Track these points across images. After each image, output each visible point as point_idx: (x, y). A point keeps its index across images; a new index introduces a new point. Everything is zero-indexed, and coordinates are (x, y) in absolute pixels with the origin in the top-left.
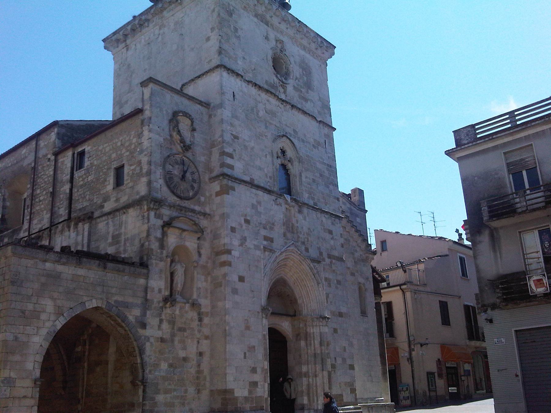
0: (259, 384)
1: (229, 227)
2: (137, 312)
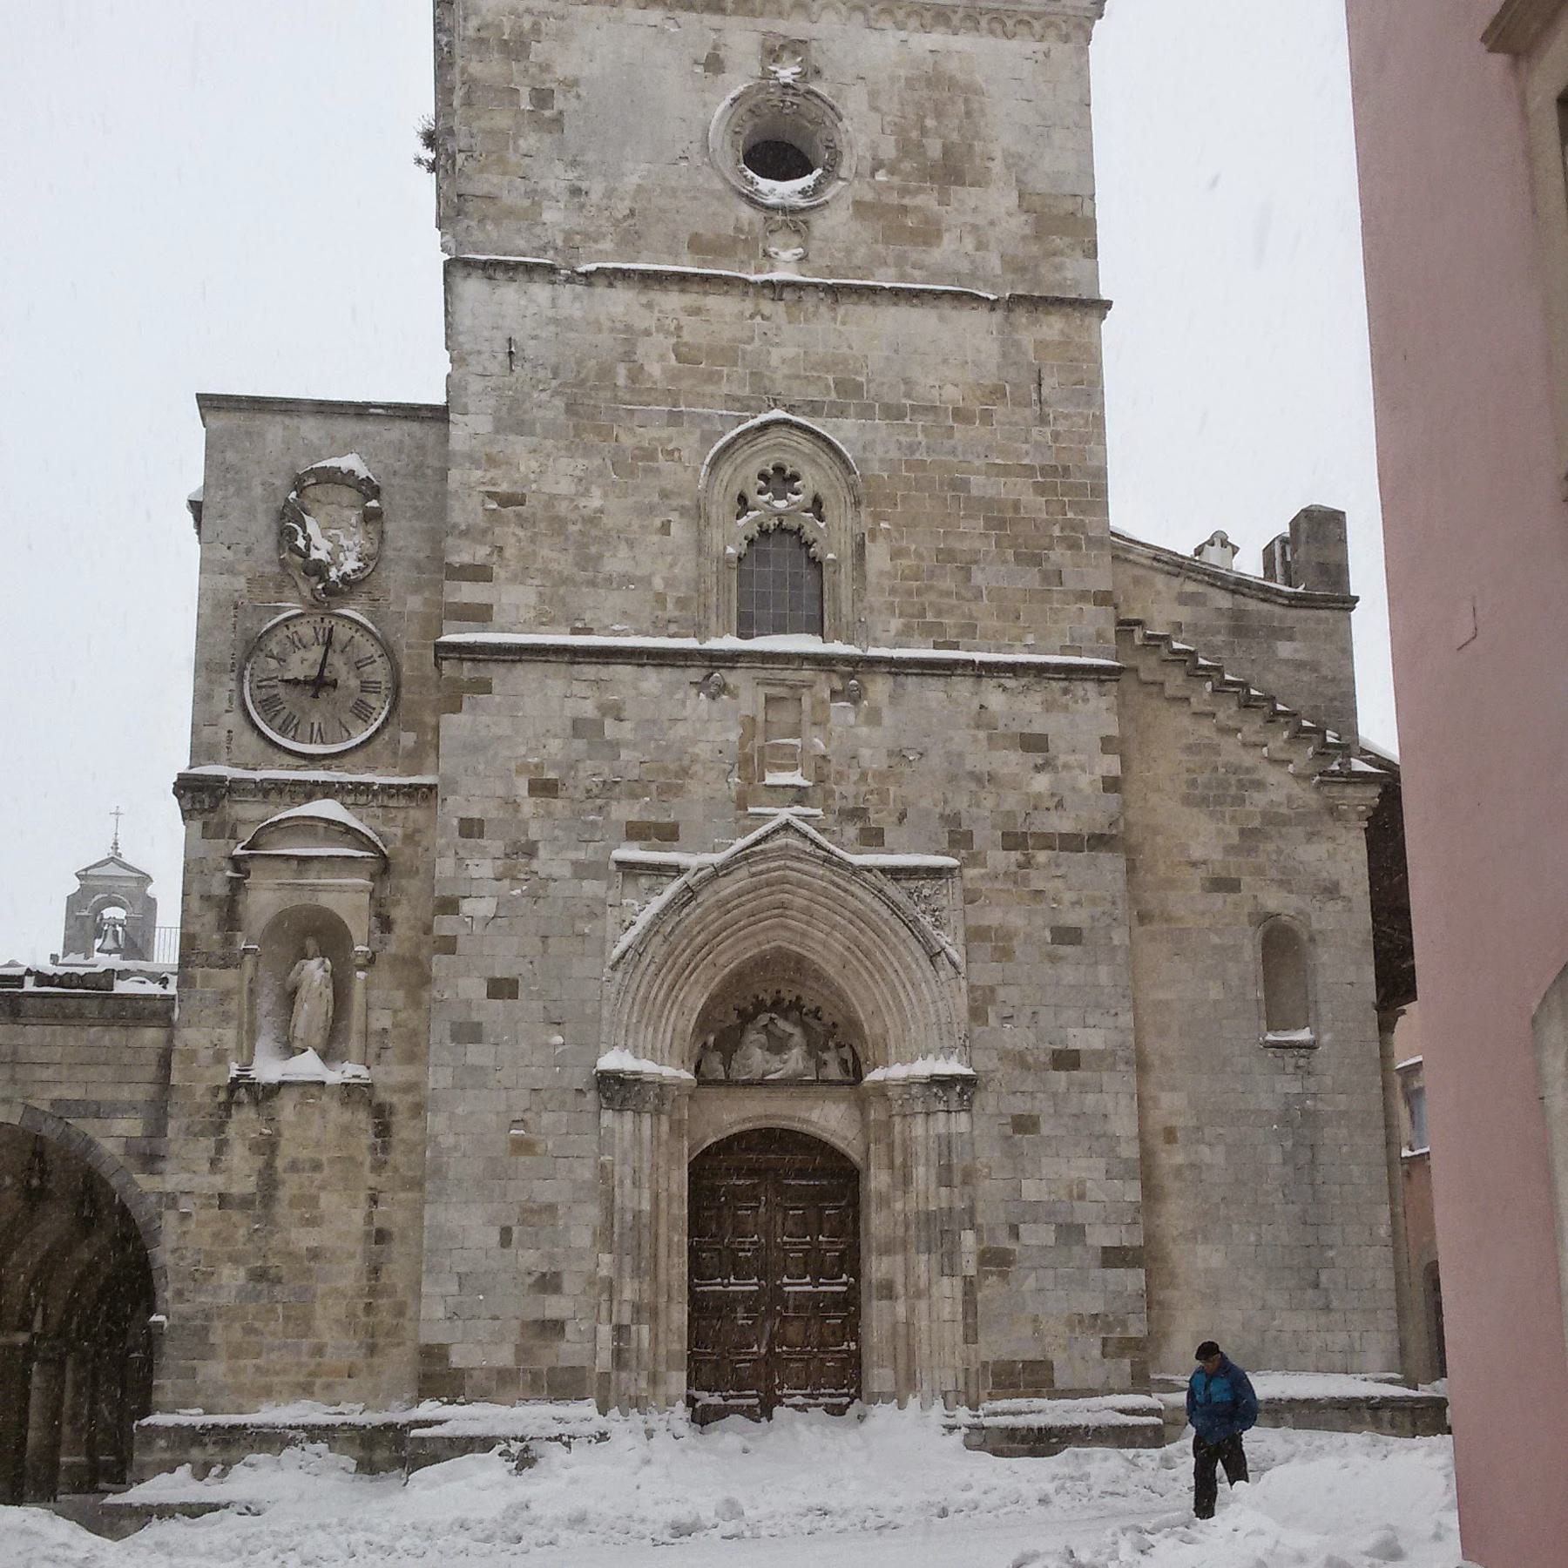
0: (569, 1328)
1: (455, 822)
2: (129, 1126)
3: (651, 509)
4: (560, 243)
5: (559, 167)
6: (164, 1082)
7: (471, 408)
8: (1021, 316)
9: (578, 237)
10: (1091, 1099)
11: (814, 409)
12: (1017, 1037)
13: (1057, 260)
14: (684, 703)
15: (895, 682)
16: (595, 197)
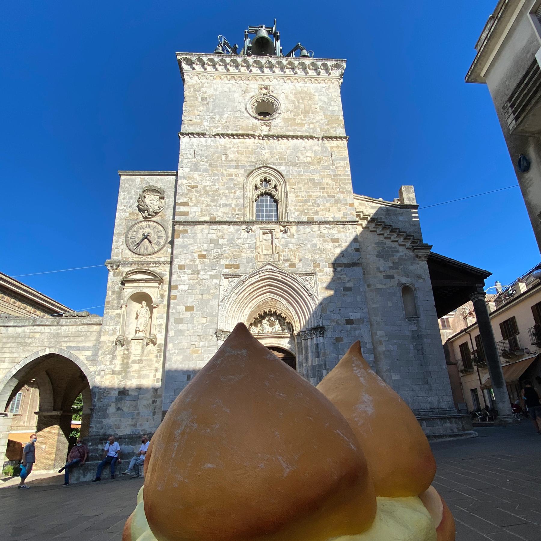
2: (89, 353)
3: (232, 188)
4: (208, 128)
5: (208, 113)
6: (98, 341)
7: (184, 166)
8: (325, 141)
9: (212, 128)
10: (357, 332)
11: (274, 163)
12: (337, 316)
13: (334, 129)
14: (240, 235)
15: (297, 227)
16: (217, 119)
